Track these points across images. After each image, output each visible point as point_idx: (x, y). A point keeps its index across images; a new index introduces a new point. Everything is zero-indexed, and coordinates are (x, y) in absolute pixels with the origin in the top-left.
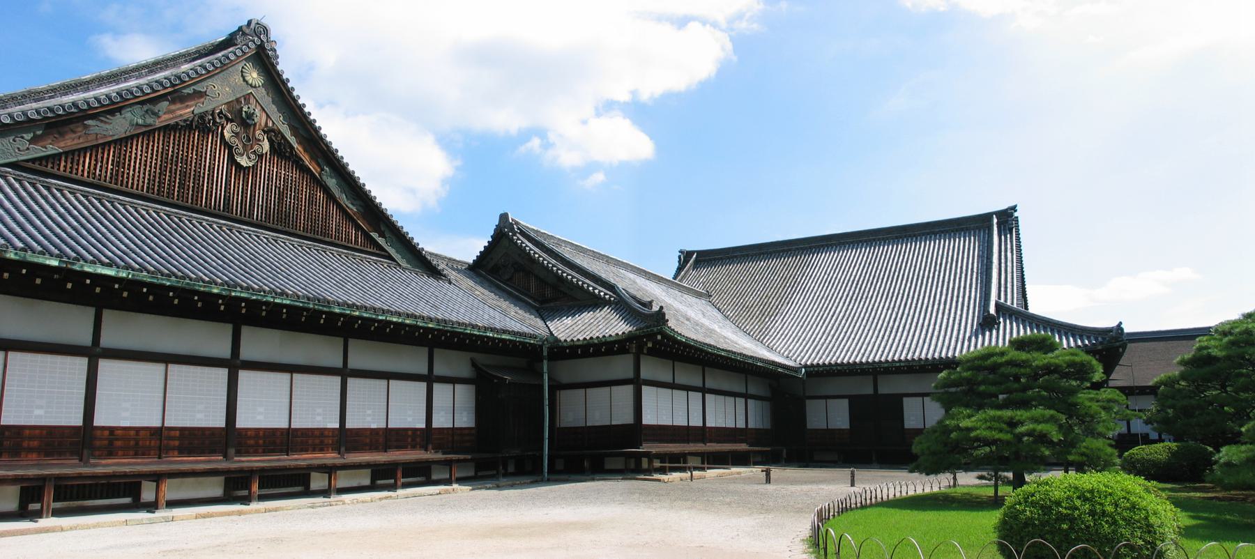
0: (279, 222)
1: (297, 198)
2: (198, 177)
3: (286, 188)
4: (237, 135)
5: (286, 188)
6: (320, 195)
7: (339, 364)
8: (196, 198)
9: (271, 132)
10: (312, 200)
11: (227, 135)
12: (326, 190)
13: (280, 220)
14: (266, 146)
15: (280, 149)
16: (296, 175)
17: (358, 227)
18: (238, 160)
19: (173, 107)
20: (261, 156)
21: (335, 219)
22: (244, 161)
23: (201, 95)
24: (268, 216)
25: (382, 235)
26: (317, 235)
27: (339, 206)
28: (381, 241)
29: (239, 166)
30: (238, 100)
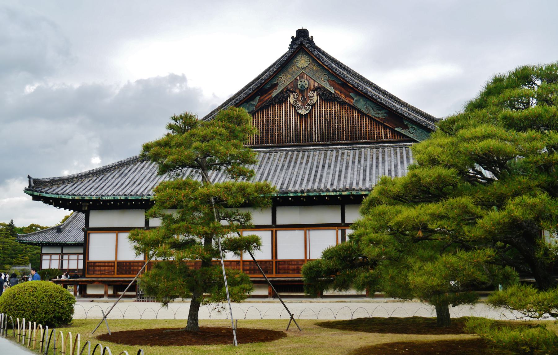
0: (331, 138)
1: (340, 122)
2: (279, 129)
3: (331, 118)
4: (297, 99)
5: (331, 118)
6: (356, 115)
7: (340, 221)
8: (281, 141)
9: (319, 89)
10: (351, 120)
11: (292, 102)
12: (359, 111)
13: (330, 139)
14: (315, 98)
15: (326, 97)
16: (336, 108)
17: (386, 127)
18: (300, 112)
19: (262, 98)
20: (313, 106)
21: (368, 126)
22: (303, 112)
23: (276, 85)
24: (322, 140)
25: (406, 127)
26: (355, 138)
27: (370, 118)
28: (404, 132)
29: (301, 116)
30: (296, 79)
